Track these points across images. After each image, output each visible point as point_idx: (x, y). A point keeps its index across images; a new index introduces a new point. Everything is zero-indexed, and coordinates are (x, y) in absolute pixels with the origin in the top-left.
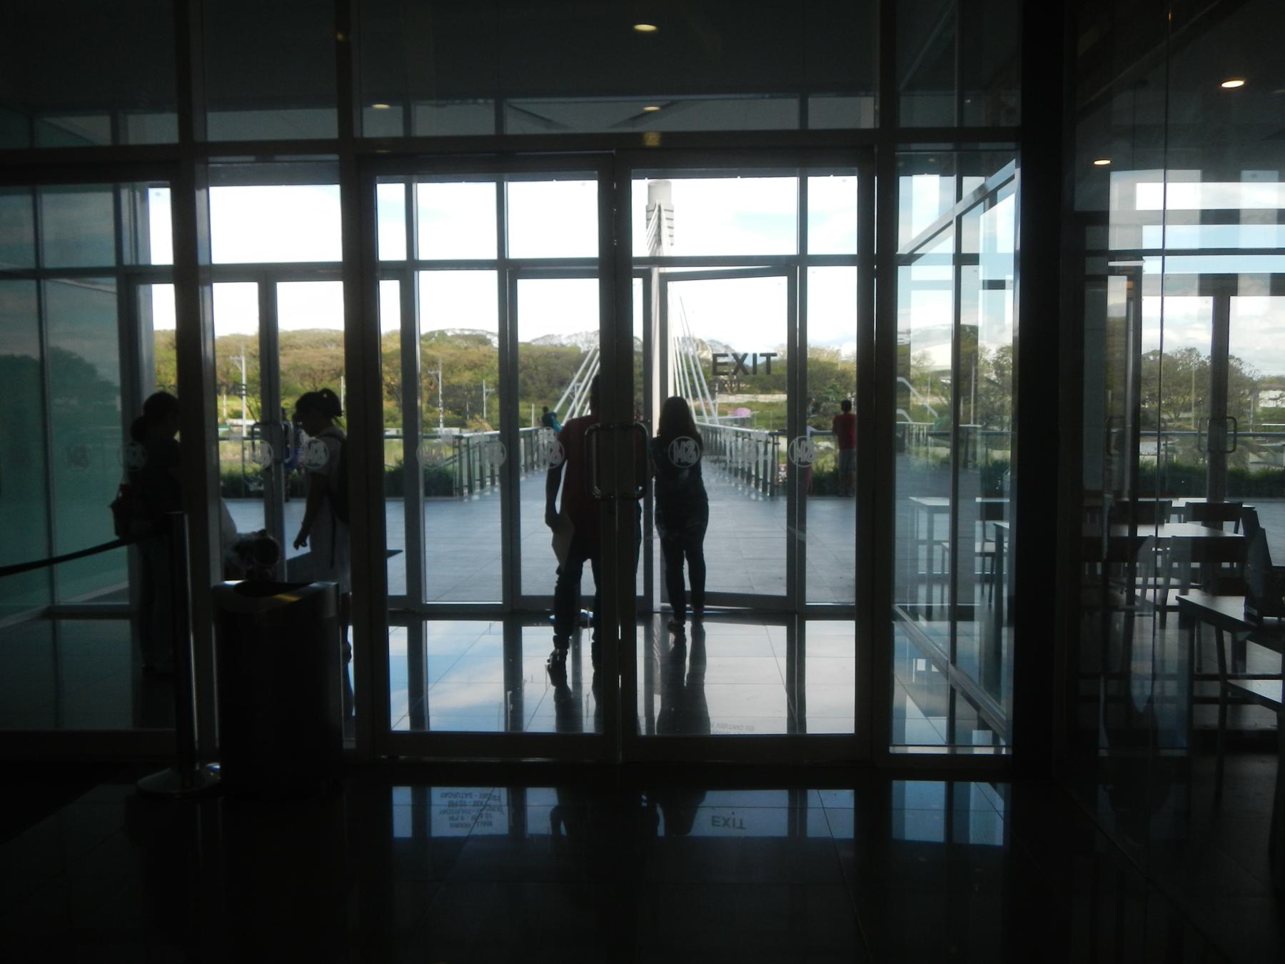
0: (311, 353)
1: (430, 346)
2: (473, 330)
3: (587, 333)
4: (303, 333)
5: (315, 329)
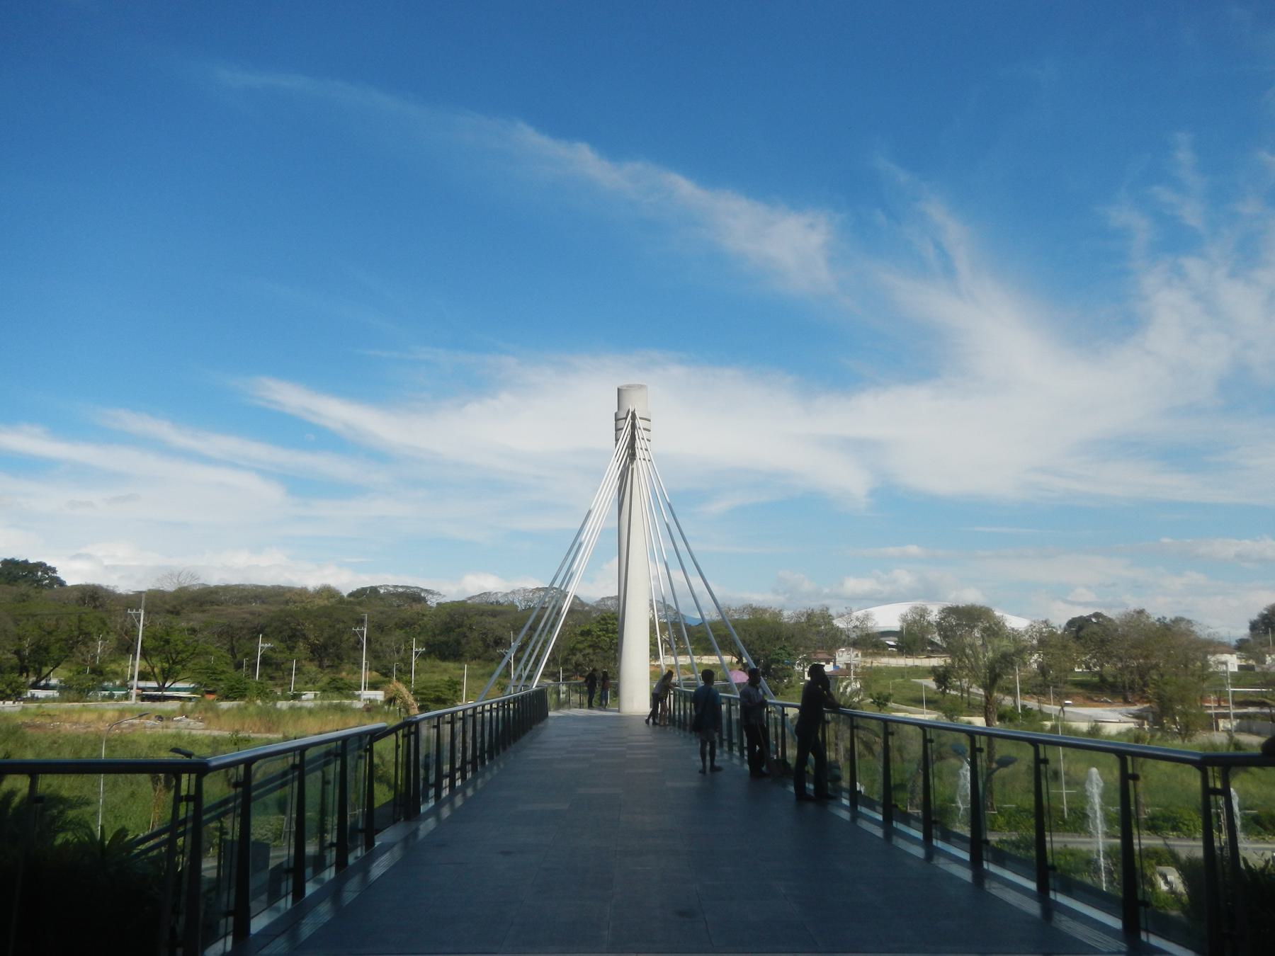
1: (360, 604)
2: (408, 587)
3: (525, 590)
4: (227, 589)
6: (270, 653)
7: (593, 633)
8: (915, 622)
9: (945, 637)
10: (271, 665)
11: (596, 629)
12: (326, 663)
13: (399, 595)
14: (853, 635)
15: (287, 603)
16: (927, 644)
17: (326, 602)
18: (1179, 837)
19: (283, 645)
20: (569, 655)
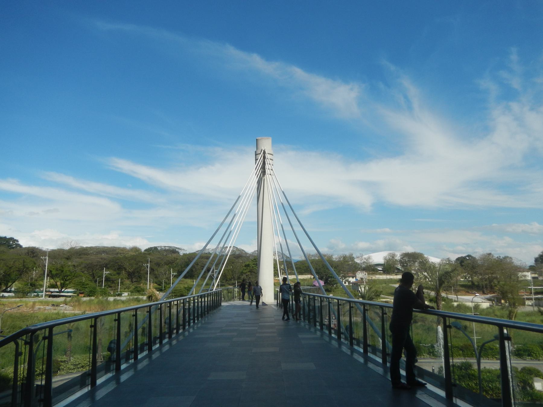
0: (93, 257)
2: (170, 247)
4: (91, 248)
5: (97, 247)
6: (109, 276)
7: (250, 266)
8: (390, 259)
9: (403, 266)
10: (110, 281)
11: (251, 264)
12: (134, 280)
13: (165, 250)
14: (363, 266)
15: (118, 253)
16: (395, 269)
17: (134, 253)
18: (531, 359)
19: (115, 273)
20: (240, 275)
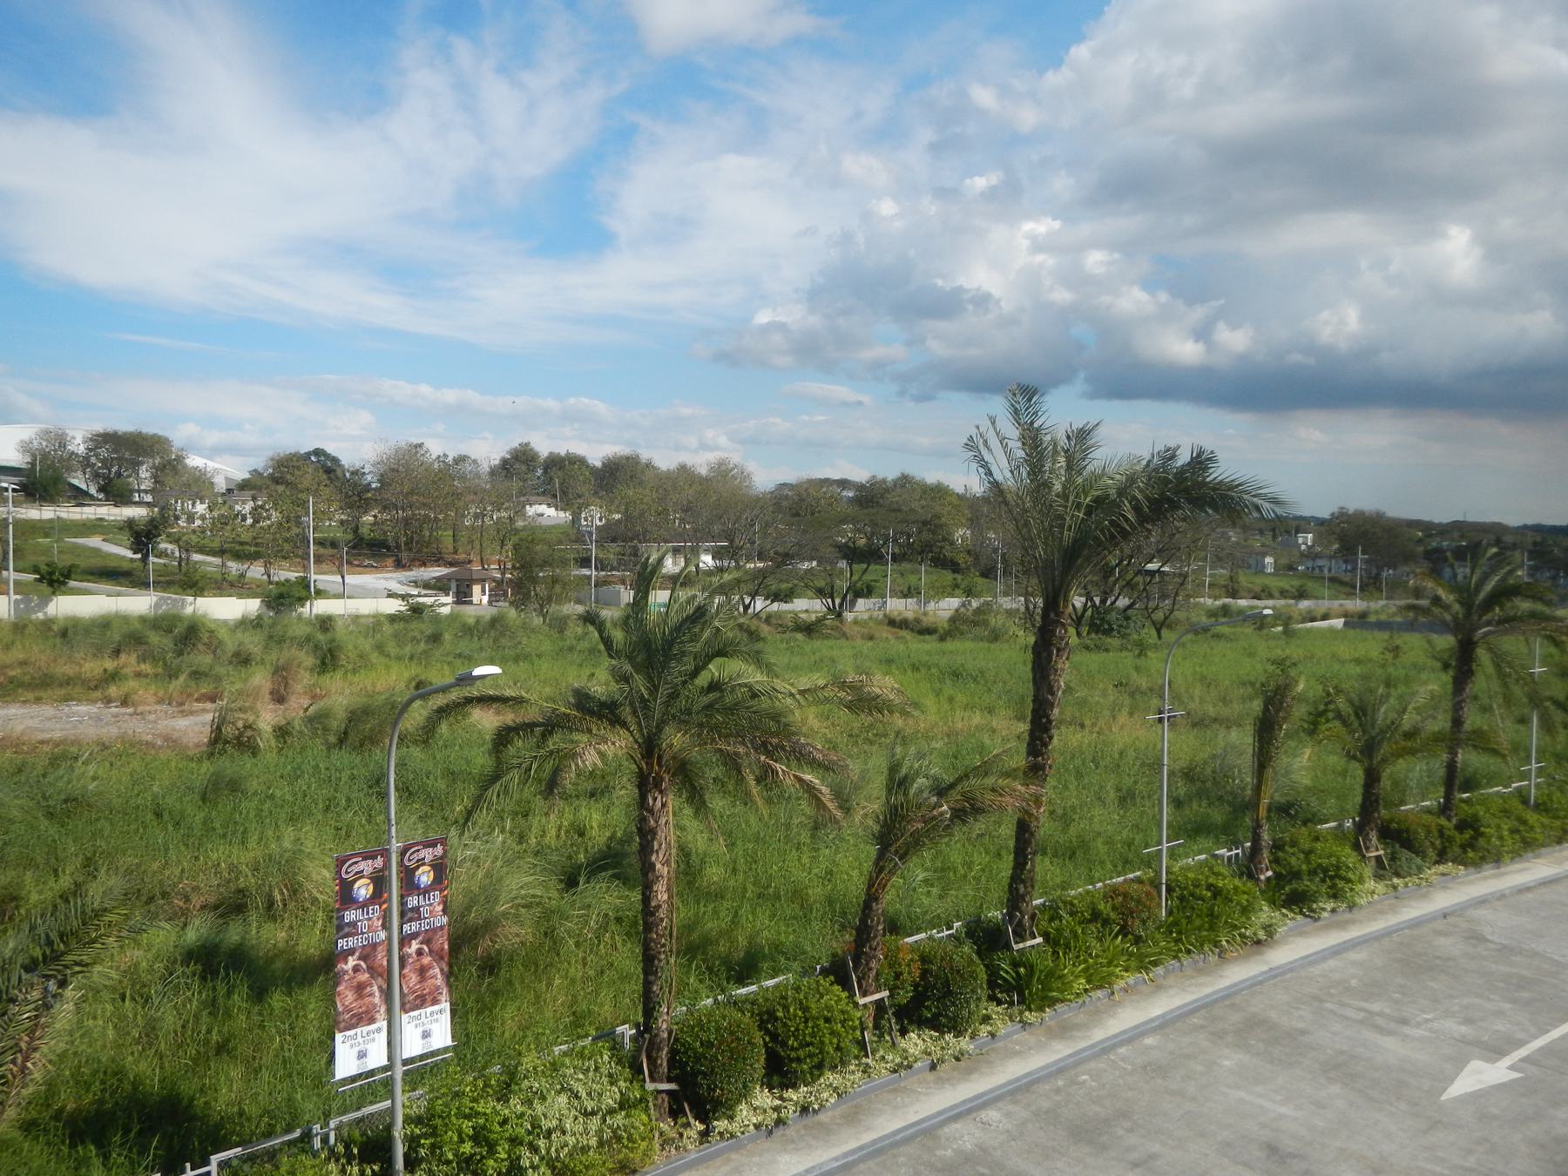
9: (96, 475)
